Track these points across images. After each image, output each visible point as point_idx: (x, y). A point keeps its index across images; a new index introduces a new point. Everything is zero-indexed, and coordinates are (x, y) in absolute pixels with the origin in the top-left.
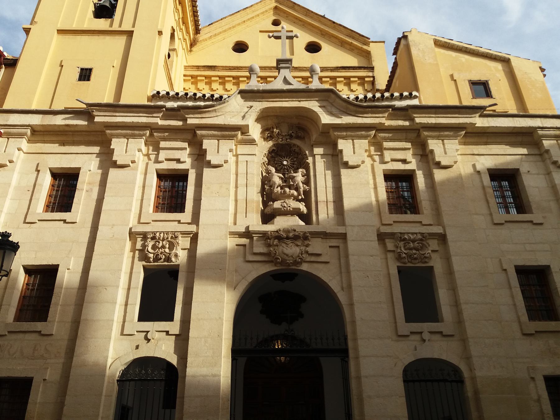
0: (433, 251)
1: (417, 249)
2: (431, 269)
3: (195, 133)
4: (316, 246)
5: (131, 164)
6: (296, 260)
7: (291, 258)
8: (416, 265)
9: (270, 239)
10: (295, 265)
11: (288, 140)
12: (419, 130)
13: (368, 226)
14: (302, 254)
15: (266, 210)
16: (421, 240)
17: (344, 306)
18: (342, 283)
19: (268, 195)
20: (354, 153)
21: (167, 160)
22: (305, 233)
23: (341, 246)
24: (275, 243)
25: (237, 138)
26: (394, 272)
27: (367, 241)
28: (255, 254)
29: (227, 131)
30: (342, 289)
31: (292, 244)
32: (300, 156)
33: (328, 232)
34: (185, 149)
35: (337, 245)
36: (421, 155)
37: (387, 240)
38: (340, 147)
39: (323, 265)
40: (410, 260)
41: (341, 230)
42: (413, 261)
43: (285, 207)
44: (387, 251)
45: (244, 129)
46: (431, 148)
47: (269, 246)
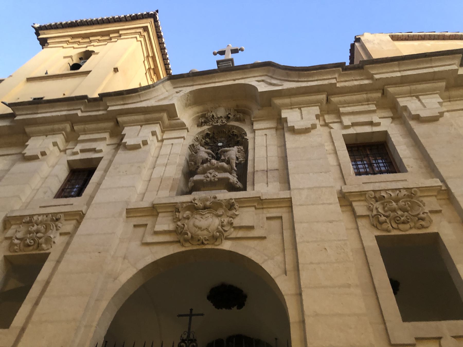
0: (431, 212)
1: (404, 210)
2: (436, 236)
3: (117, 122)
5: (40, 156)
7: (205, 232)
8: (407, 233)
9: (179, 212)
10: (213, 244)
12: (383, 90)
13: (323, 187)
14: (222, 226)
16: (409, 196)
17: (286, 297)
20: (302, 118)
21: (82, 151)
23: (286, 217)
25: (163, 122)
26: (371, 243)
27: (323, 204)
28: (156, 233)
29: (151, 115)
33: (263, 198)
34: (104, 139)
35: (279, 215)
36: (392, 118)
37: (354, 204)
38: (283, 116)
39: (256, 242)
40: (395, 225)
42: (401, 226)
43: (208, 177)
44: (356, 216)
45: (170, 110)
46: (402, 104)
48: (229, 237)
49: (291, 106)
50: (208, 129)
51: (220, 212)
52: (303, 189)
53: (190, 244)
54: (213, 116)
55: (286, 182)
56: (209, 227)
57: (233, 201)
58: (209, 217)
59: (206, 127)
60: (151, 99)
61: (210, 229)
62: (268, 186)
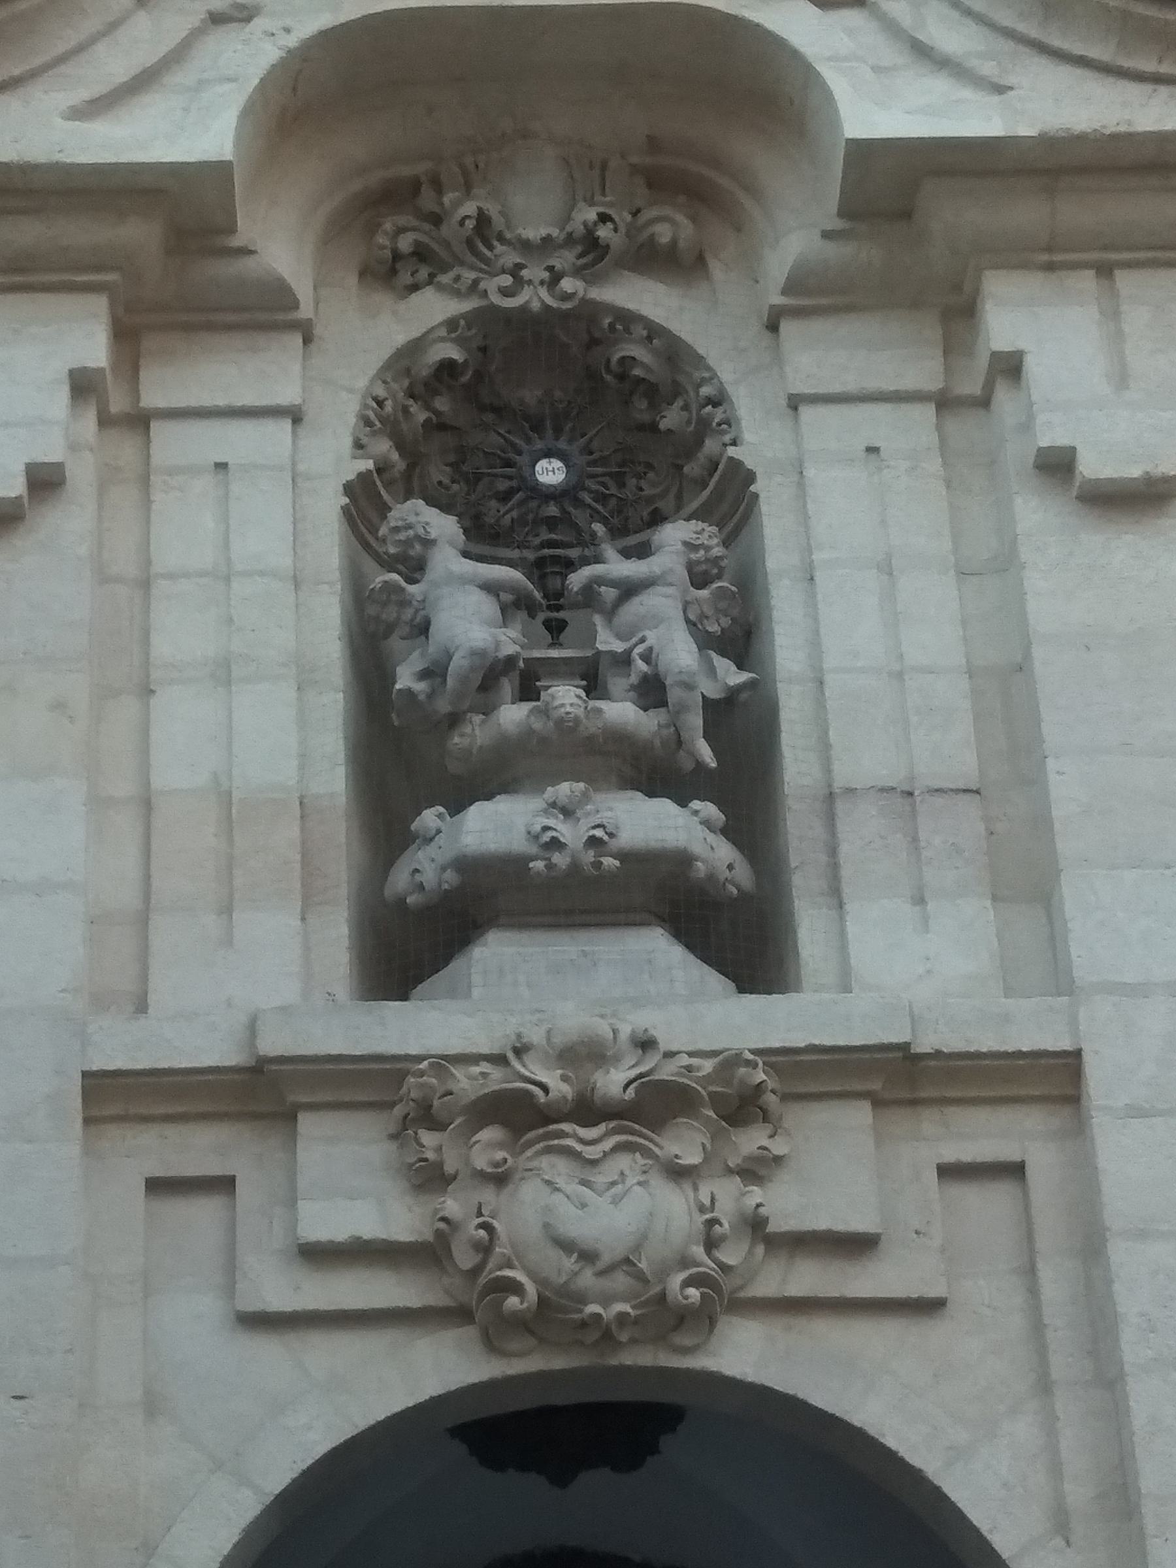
4: (832, 1169)
6: (662, 1297)
7: (621, 1281)
10: (660, 1339)
11: (568, 284)
14: (711, 1244)
15: (399, 880)
18: (1056, 1470)
19: (404, 752)
22: (731, 1062)
24: (481, 1161)
30: (1061, 1523)
31: (624, 1161)
32: (671, 418)
33: (924, 1045)
41: (1033, 1030)
43: (556, 844)
47: (430, 1179)
48: (742, 1294)
49: (1049, 256)
50: (451, 324)
51: (685, 1144)
52: (1140, 990)
53: (532, 1342)
54: (483, 220)
55: (1026, 881)
56: (637, 1248)
57: (760, 1076)
58: (631, 1180)
59: (432, 309)
60: (33, 75)
61: (643, 1265)
62: (925, 920)
